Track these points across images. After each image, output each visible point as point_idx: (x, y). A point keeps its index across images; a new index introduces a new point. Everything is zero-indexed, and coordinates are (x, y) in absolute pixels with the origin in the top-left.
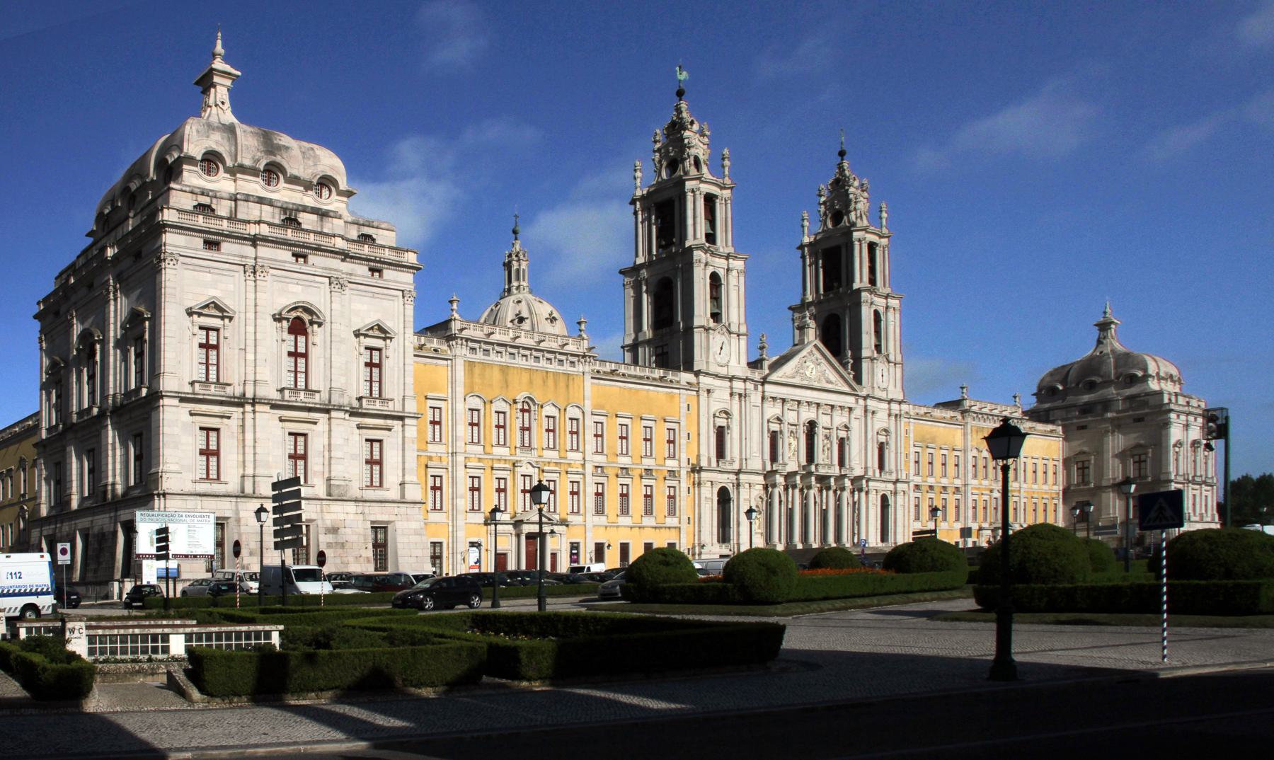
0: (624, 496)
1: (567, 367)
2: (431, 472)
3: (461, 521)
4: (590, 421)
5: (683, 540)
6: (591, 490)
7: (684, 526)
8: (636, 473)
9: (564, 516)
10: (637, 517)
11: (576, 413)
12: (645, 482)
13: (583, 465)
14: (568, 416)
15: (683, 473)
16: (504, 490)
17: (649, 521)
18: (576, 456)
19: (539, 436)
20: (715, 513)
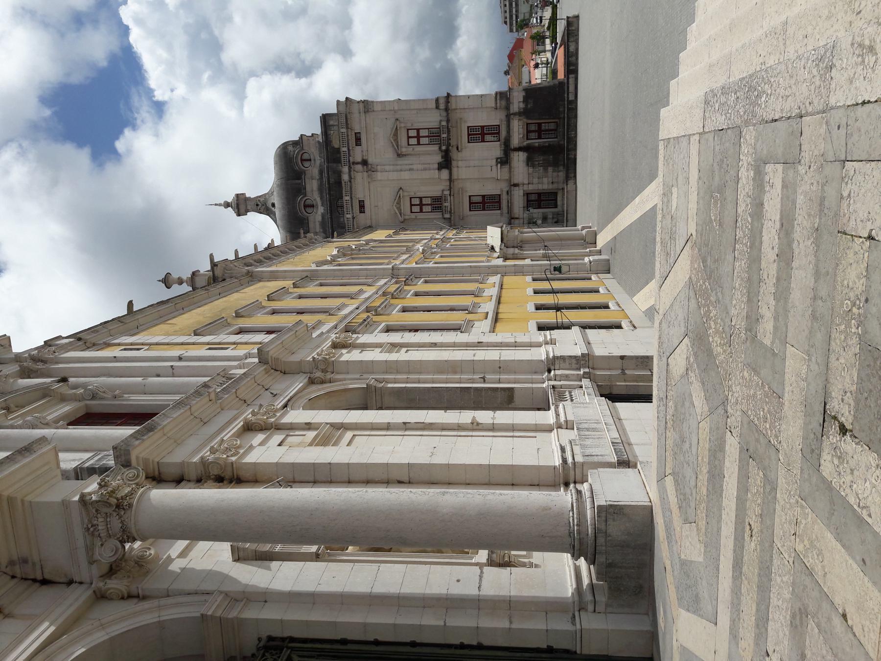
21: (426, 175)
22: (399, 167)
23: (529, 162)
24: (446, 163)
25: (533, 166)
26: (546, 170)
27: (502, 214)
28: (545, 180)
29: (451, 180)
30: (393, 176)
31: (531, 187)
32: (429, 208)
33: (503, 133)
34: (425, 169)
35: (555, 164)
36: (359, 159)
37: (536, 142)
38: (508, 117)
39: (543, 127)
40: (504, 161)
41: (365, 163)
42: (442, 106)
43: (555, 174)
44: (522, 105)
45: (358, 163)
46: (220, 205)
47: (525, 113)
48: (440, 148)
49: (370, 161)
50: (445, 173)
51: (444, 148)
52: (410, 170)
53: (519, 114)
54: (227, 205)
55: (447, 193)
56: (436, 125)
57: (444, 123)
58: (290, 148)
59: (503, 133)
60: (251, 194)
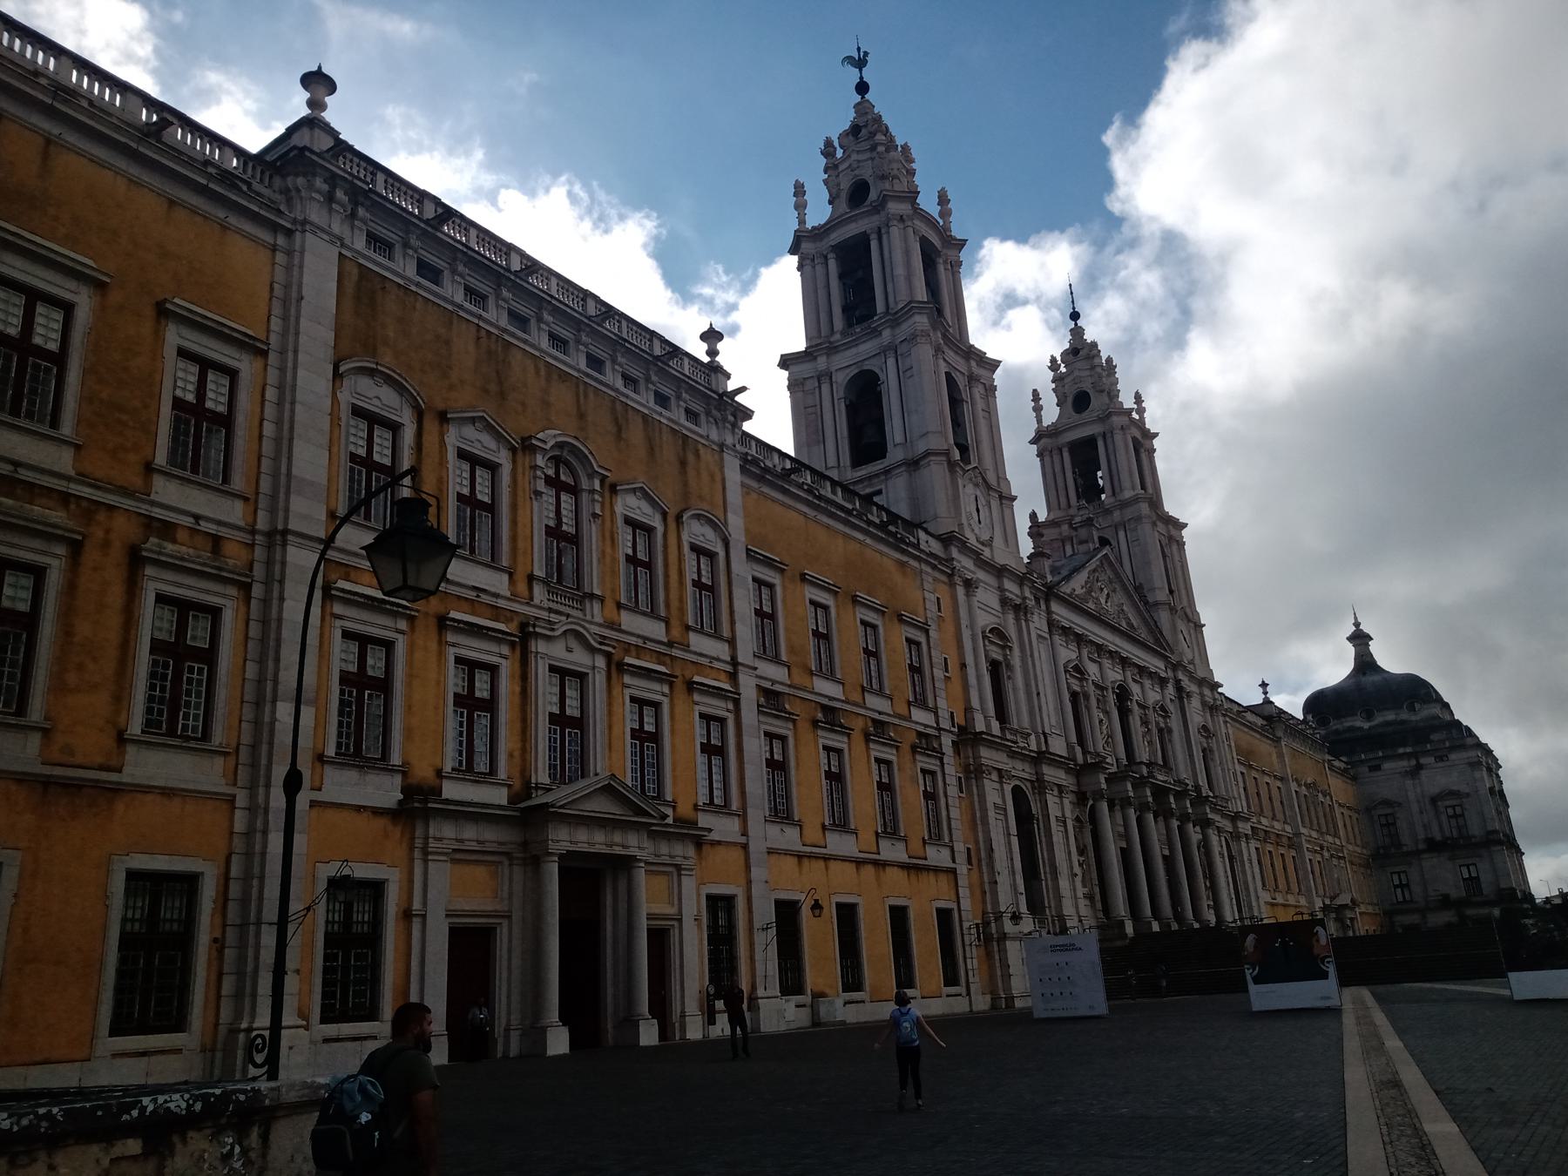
0: (835, 778)
2: (154, 583)
4: (743, 570)
5: (966, 904)
6: (755, 748)
7: (962, 869)
8: (858, 724)
9: (685, 809)
10: (867, 837)
11: (706, 536)
12: (878, 751)
13: (733, 677)
14: (685, 537)
15: (947, 741)
16: (490, 705)
17: (892, 851)
19: (603, 565)
20: (1015, 841)
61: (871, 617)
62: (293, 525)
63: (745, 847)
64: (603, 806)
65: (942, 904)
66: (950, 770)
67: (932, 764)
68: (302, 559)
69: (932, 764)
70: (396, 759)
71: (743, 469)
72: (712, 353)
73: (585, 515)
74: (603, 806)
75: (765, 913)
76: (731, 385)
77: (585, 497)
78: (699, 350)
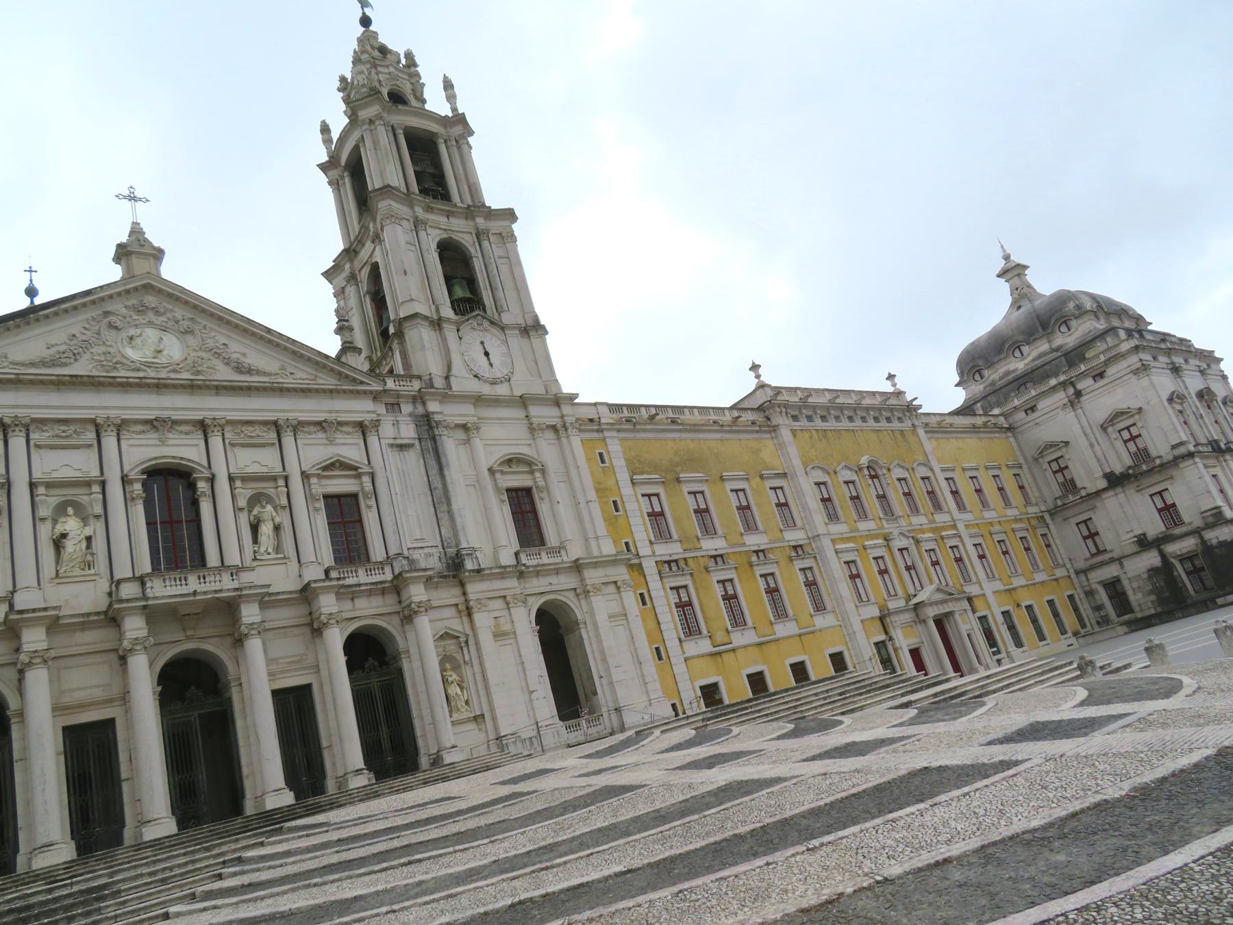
1: (896, 425)
3: (856, 622)
13: (955, 527)
18: (941, 518)
21: (1093, 464)
22: (1089, 431)
23: (1153, 571)
24: (1115, 481)
25: (1150, 577)
26: (1151, 592)
27: (1086, 560)
28: (1139, 595)
29: (1098, 493)
30: (1077, 429)
31: (1125, 582)
32: (1061, 479)
33: (1178, 531)
34: (1098, 461)
35: (1161, 601)
36: (1080, 386)
37: (1180, 570)
38: (1197, 532)
39: (1203, 574)
40: (1143, 543)
41: (1078, 394)
42: (1178, 452)
43: (1150, 605)
44: (1214, 542)
45: (1074, 387)
46: (1004, 250)
47: (1207, 548)
48: (1130, 467)
49: (1083, 399)
50: (1103, 484)
51: (1131, 471)
52: (1092, 446)
53: (1203, 542)
54: (1007, 258)
55: (1083, 493)
56: (1153, 453)
57: (1158, 462)
58: (1071, 305)
59: (1178, 531)
60: (1031, 277)
61: (996, 472)
62: (820, 532)
63: (984, 595)
64: (939, 596)
65: (1070, 593)
66: (1053, 531)
67: (1045, 531)
68: (826, 542)
69: (1045, 531)
70: (873, 600)
71: (926, 432)
72: (894, 385)
73: (885, 486)
74: (939, 596)
75: (1000, 619)
76: (909, 397)
77: (882, 478)
78: (887, 387)
